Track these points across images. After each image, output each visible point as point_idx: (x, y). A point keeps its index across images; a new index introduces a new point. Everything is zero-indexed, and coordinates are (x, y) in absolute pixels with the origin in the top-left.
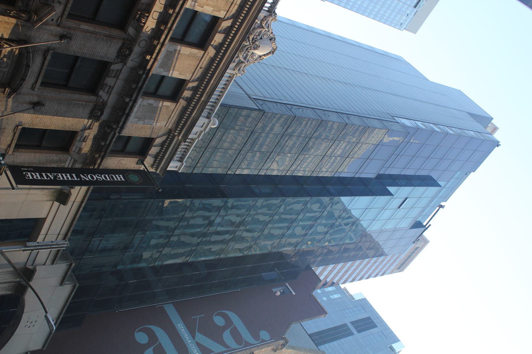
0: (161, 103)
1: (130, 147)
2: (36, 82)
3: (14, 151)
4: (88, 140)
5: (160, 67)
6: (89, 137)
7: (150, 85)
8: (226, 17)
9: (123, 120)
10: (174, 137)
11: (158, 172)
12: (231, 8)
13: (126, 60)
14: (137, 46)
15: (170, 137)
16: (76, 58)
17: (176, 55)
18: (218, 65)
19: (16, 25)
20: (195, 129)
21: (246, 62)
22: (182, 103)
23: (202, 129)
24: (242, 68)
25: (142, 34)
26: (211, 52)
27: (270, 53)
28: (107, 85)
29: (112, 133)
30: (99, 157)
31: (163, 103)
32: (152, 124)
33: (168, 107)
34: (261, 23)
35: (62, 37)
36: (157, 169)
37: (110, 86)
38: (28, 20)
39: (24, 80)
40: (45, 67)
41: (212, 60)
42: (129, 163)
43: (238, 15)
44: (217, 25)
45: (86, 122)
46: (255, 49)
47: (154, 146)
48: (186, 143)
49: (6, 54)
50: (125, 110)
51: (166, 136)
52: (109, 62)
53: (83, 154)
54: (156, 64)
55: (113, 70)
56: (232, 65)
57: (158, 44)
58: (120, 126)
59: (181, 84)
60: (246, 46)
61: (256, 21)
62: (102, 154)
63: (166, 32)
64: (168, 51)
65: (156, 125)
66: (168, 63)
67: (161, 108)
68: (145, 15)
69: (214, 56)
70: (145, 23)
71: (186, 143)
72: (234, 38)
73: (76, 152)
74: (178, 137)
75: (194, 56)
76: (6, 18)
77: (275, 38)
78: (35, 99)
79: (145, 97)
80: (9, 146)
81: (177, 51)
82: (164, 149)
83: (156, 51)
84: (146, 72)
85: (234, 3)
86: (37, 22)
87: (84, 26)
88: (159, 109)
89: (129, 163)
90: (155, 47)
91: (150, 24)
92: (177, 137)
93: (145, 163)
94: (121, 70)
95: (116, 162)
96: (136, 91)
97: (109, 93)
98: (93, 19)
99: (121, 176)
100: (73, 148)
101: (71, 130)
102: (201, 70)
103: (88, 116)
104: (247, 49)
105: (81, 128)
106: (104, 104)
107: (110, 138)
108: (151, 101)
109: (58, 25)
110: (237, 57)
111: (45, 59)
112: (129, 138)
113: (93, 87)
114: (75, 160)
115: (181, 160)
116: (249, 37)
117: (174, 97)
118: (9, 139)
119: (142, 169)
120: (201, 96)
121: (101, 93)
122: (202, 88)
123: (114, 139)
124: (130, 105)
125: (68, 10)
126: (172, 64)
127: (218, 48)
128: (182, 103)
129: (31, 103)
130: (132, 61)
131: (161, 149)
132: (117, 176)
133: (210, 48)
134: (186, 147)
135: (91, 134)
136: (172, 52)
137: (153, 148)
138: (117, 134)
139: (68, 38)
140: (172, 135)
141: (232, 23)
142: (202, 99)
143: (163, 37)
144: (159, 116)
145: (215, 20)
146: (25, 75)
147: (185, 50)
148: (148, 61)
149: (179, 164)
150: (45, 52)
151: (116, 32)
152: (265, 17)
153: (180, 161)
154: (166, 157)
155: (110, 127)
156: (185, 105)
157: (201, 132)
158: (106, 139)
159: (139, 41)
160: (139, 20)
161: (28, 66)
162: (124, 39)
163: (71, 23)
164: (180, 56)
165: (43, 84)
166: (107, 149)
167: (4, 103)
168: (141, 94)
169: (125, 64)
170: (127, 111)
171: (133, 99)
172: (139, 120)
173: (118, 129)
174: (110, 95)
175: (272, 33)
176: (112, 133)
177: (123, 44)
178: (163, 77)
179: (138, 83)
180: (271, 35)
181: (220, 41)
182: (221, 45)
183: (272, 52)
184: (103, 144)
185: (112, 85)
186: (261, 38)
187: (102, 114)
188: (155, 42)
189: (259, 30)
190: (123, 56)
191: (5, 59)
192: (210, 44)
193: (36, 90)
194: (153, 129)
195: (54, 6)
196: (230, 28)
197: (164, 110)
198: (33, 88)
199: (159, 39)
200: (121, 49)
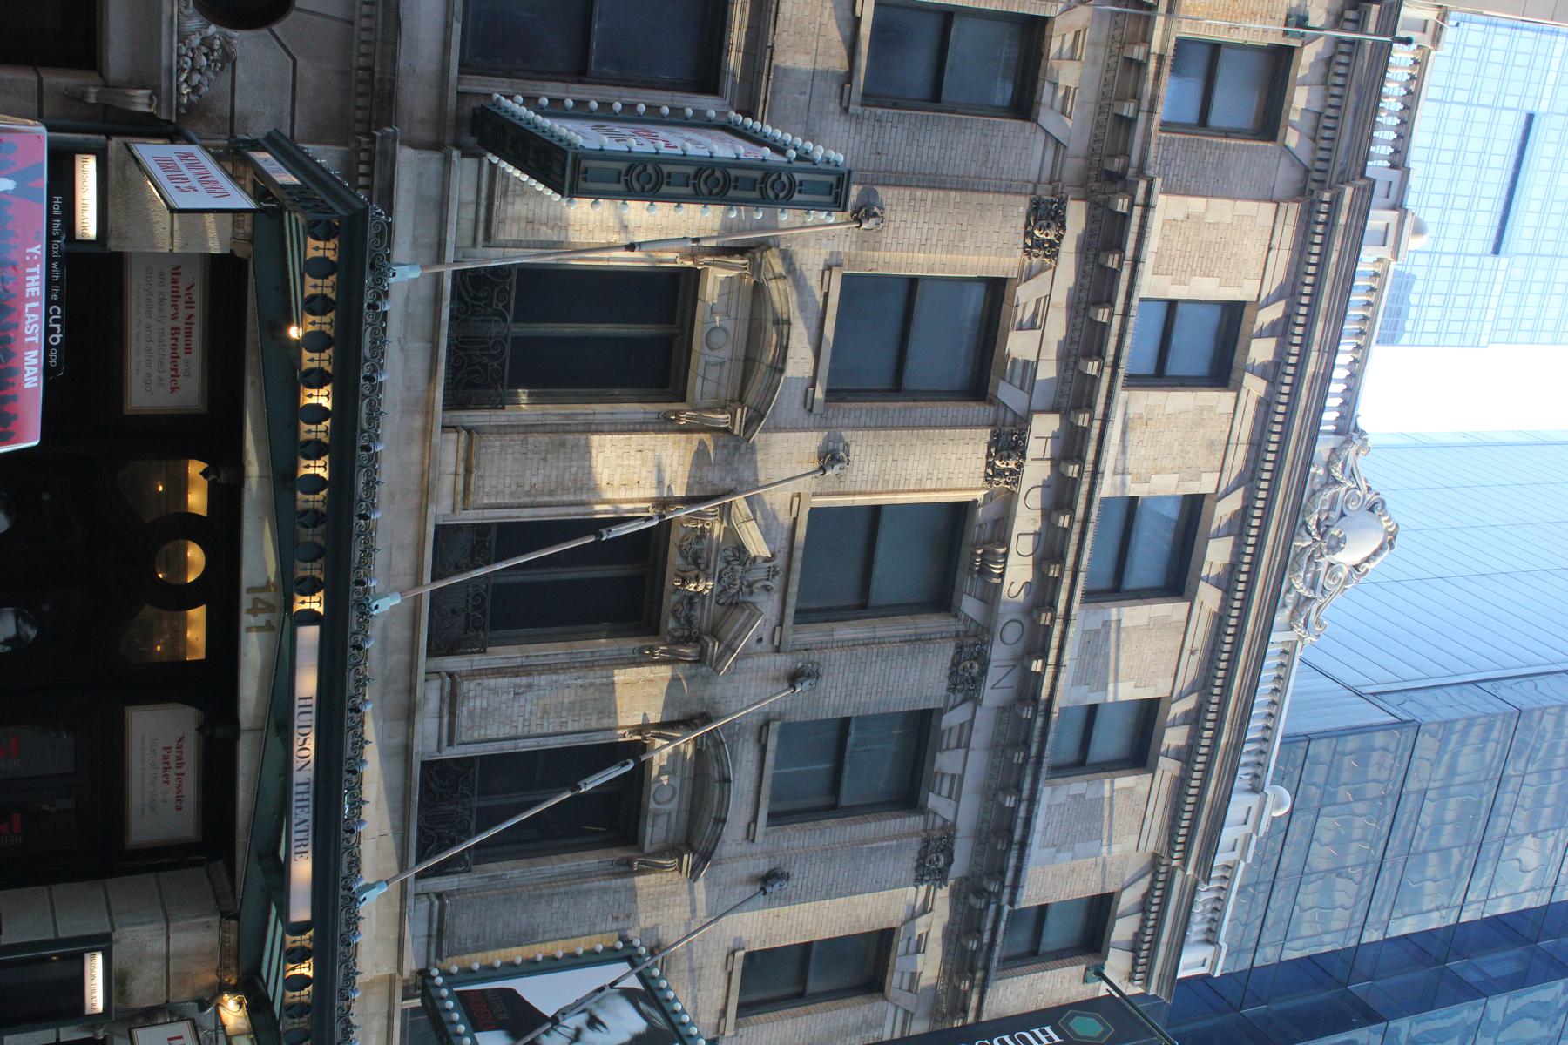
0: (1107, 786)
1: (1053, 936)
2: (755, 819)
3: (737, 1026)
4: (929, 947)
5: (1080, 679)
6: (931, 936)
7: (1060, 744)
8: (1222, 489)
9: (1012, 862)
10: (1171, 874)
11: (1152, 992)
12: (1229, 459)
13: (977, 690)
14: (997, 641)
15: (1161, 877)
16: (845, 722)
17: (1113, 635)
18: (1241, 627)
19: (675, 680)
20: (1228, 835)
21: (1318, 595)
22: (1168, 768)
23: (1248, 828)
24: (1312, 618)
25: (1002, 608)
26: (1209, 598)
27: (1381, 548)
29: (993, 907)
30: (972, 986)
31: (1112, 783)
32: (1098, 854)
33: (1131, 789)
34: (1328, 471)
35: (794, 678)
36: (1147, 982)
37: (953, 776)
38: (701, 659)
39: (724, 821)
40: (768, 772)
41: (1220, 620)
42: (1062, 984)
43: (1253, 471)
44: (1203, 517)
45: (912, 894)
46: (1333, 549)
47: (1121, 916)
48: (1214, 884)
49: (664, 763)
50: (1011, 832)
51: (1148, 878)
52: (931, 710)
53: (925, 989)
54: (1063, 677)
56: (1281, 617)
57: (1053, 620)
58: (1008, 881)
59: (1148, 713)
60: (1303, 549)
61: (1313, 470)
62: (979, 975)
63: (1066, 581)
64: (1085, 633)
65: (1109, 852)
66: (1097, 664)
67: (1111, 798)
68: (995, 554)
69: (1221, 608)
70: (1002, 576)
71: (1214, 884)
72: (1261, 538)
73: (905, 986)
74: (1185, 871)
75: (1163, 624)
76: (645, 671)
77: (1383, 502)
78: (763, 866)
79: (1059, 781)
80: (723, 1013)
81: (1113, 625)
82: (1152, 916)
83: (1055, 642)
84: (1041, 707)
85: (1233, 440)
86: (721, 658)
87: (845, 631)
88: (1106, 801)
89: (1062, 984)
90: (1048, 630)
91: (1018, 572)
92: (1179, 872)
93: (1106, 973)
94: (972, 721)
95: (1024, 991)
96: (1029, 771)
97: (955, 795)
98: (862, 606)
99: (1047, 1029)
100: (894, 980)
101: (877, 927)
102: (1195, 659)
103: (913, 875)
104: (1310, 558)
105: (902, 915)
106: (949, 830)
107: (989, 925)
108: (1078, 785)
109: (777, 650)
110: (1288, 591)
111: (763, 750)
112: (1043, 910)
113: (907, 794)
114: (906, 1012)
115: (1210, 939)
116: (1305, 523)
117: (1139, 756)
118: (721, 992)
119: (1103, 993)
120: (1217, 732)
121: (933, 801)
122: (1213, 707)
123: (1002, 925)
124: (1022, 813)
125: (792, 601)
126: (1107, 664)
127: (1226, 582)
128: (1168, 768)
129: (754, 879)
130: (996, 688)
131: (1144, 920)
132: (1036, 1031)
133: (1203, 586)
134: (1214, 895)
135: (935, 924)
136: (1097, 632)
137: (1118, 922)
138: (1007, 908)
139: (809, 676)
140: (1163, 869)
141: (1244, 498)
142: (1224, 740)
143: (1063, 596)
144: (1111, 825)
145: (1194, 506)
146: (724, 804)
147: (1134, 615)
148: (1039, 676)
149: (1208, 952)
150: (761, 728)
151: (931, 623)
152: (1334, 450)
153: (1208, 942)
154: (1165, 938)
155: (980, 892)
156: (1177, 773)
157: (1248, 837)
158: (980, 932)
160: (984, 571)
161: (725, 780)
162: (957, 636)
163: (810, 634)
164: (1123, 635)
165: (775, 818)
166: (989, 959)
167: (686, 896)
168: (1043, 776)
169: (977, 702)
170: (1017, 835)
171: (1025, 794)
172: (1058, 851)
173: (1007, 891)
174: (958, 801)
175: (1369, 489)
176: (993, 907)
177: (960, 649)
178: (1093, 710)
179: (1026, 744)
180: (1369, 497)
181: (1227, 560)
182: (1232, 568)
183: (1389, 542)
184: (973, 945)
185: (957, 770)
186: (1343, 515)
187: (949, 862)
188: (1045, 618)
189: (1328, 494)
190: (965, 682)
191: (665, 779)
192: (1199, 578)
193: (759, 839)
194: (1104, 865)
195: (754, 604)
196: (1245, 512)
197: (1119, 802)
198: (750, 836)
199: (1052, 606)
200: (955, 664)
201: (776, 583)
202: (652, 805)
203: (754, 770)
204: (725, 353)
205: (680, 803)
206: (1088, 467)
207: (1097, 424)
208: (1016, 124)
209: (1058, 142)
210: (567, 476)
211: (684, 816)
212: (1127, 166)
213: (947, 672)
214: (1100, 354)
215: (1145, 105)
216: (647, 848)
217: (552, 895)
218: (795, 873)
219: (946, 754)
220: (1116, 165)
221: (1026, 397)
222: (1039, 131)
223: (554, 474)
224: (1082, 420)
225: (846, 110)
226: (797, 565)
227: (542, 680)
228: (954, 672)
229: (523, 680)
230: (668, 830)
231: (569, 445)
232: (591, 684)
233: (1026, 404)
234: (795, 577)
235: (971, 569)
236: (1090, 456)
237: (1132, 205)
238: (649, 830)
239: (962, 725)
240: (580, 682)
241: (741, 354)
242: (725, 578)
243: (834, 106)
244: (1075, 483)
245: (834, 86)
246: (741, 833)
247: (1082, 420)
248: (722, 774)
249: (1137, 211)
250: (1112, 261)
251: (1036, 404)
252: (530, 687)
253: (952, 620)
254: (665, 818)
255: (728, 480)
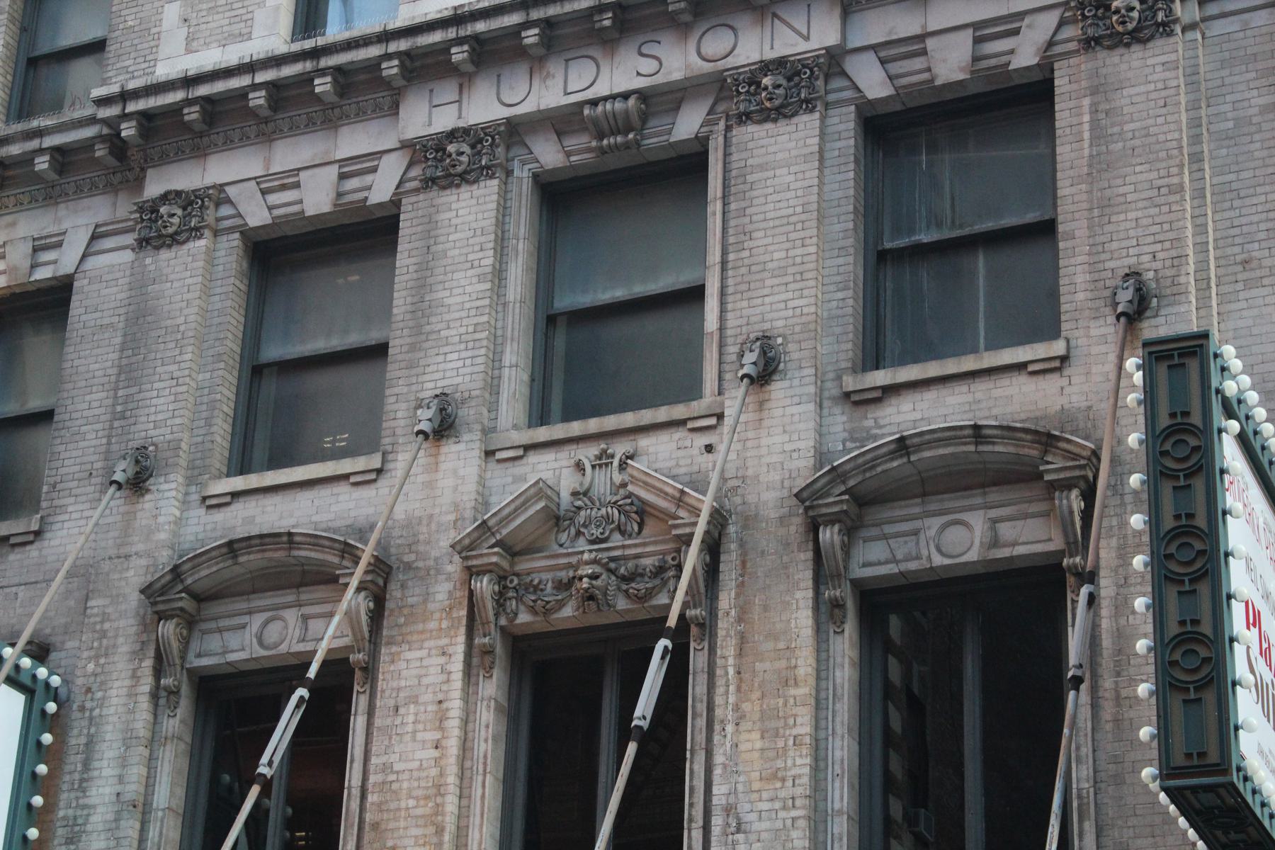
2: (1020, 367)
14: (731, 62)
28: (976, 59)
37: (978, 41)
39: (976, 427)
55: (890, 78)
94: (874, 48)
103: (1159, 43)
121: (1024, 54)
146: (951, 435)
150: (857, 403)
159: (708, 67)
161: (902, 445)
174: (1021, 15)
177: (745, 118)
185: (967, 37)
201: (620, 448)
202: (972, 556)
203: (930, 395)
204: (291, 616)
205: (971, 508)
206: (452, 33)
207: (393, 47)
208: (75, 302)
209: (95, 237)
210: (419, 811)
211: (994, 495)
212: (100, 138)
213: (783, 126)
214: (306, 80)
215: (34, 144)
216: (1057, 544)
217: (1117, 698)
218: (1123, 264)
219: (935, 70)
220: (100, 152)
221: (385, 158)
222: (83, 268)
223: (415, 831)
224: (391, 69)
225: (38, 534)
226: (593, 425)
227: (720, 790)
228: (779, 113)
229: (717, 821)
230: (1026, 516)
231: (377, 818)
232: (737, 708)
233: (393, 156)
234: (611, 422)
235: (627, 146)
236: (436, 37)
237: (125, 116)
238: (1020, 550)
239: (883, 62)
240: (730, 728)
241: (290, 598)
242: (597, 532)
243: (33, 552)
244: (477, 41)
245: (12, 557)
246: (1051, 384)
247: (391, 69)
248: (893, 455)
249: (132, 107)
250: (192, 114)
251: (391, 143)
252: (728, 810)
253: (712, 144)
254: (1006, 531)
255: (450, 568)
